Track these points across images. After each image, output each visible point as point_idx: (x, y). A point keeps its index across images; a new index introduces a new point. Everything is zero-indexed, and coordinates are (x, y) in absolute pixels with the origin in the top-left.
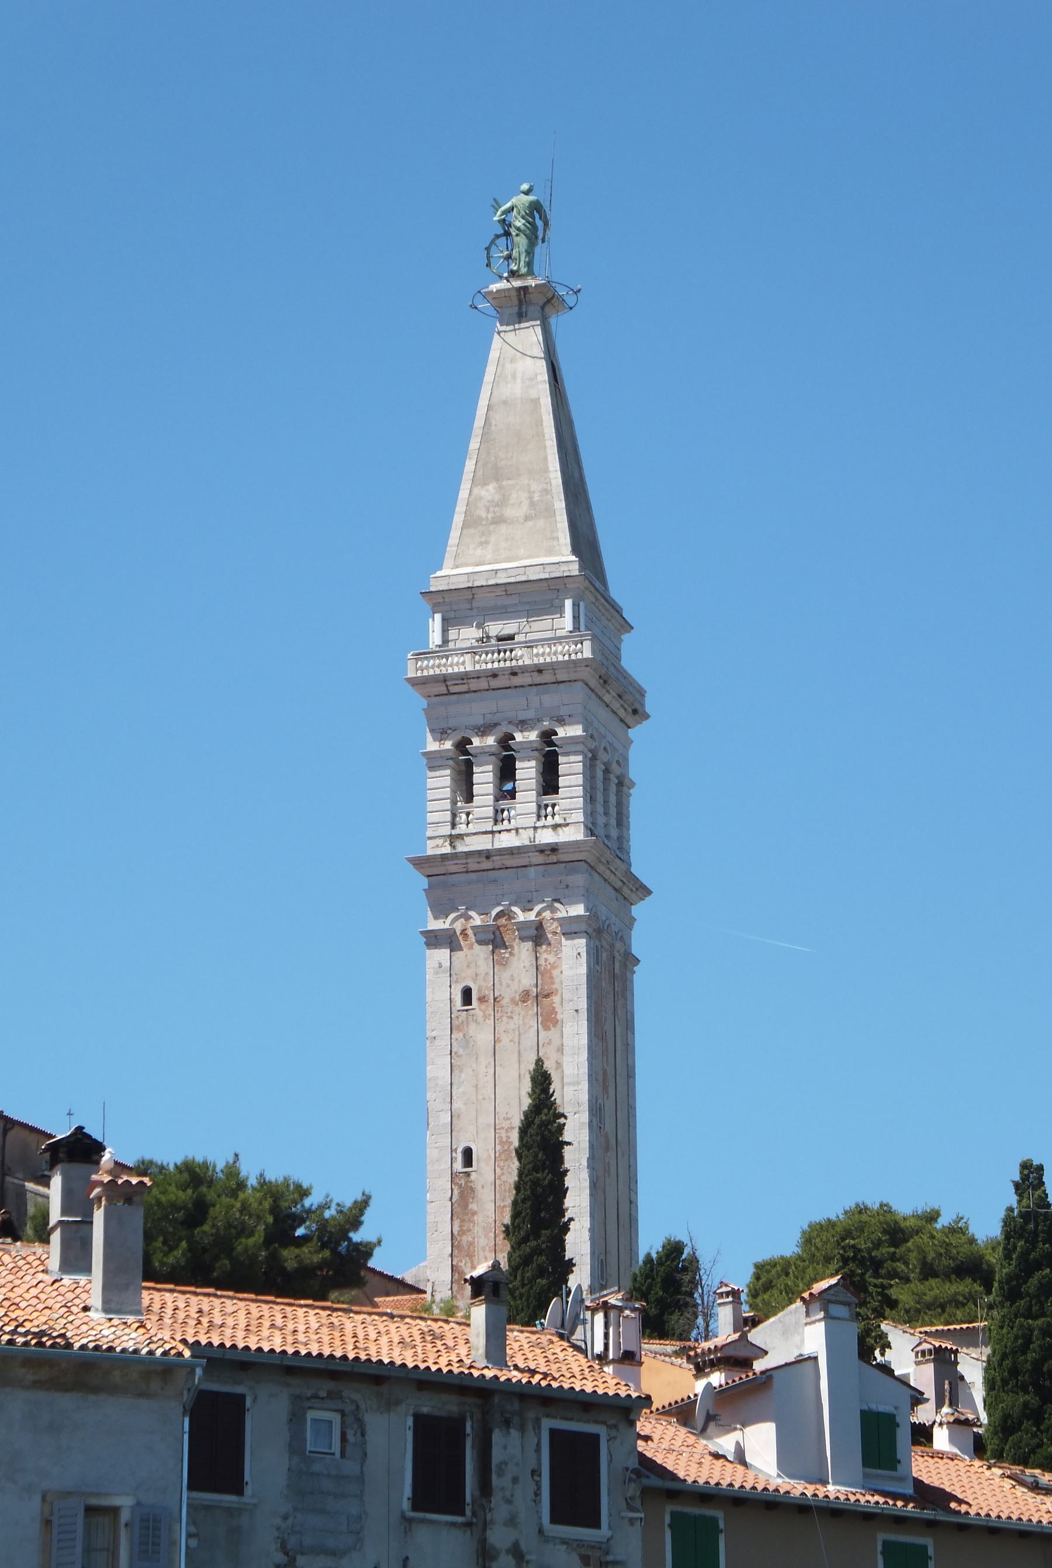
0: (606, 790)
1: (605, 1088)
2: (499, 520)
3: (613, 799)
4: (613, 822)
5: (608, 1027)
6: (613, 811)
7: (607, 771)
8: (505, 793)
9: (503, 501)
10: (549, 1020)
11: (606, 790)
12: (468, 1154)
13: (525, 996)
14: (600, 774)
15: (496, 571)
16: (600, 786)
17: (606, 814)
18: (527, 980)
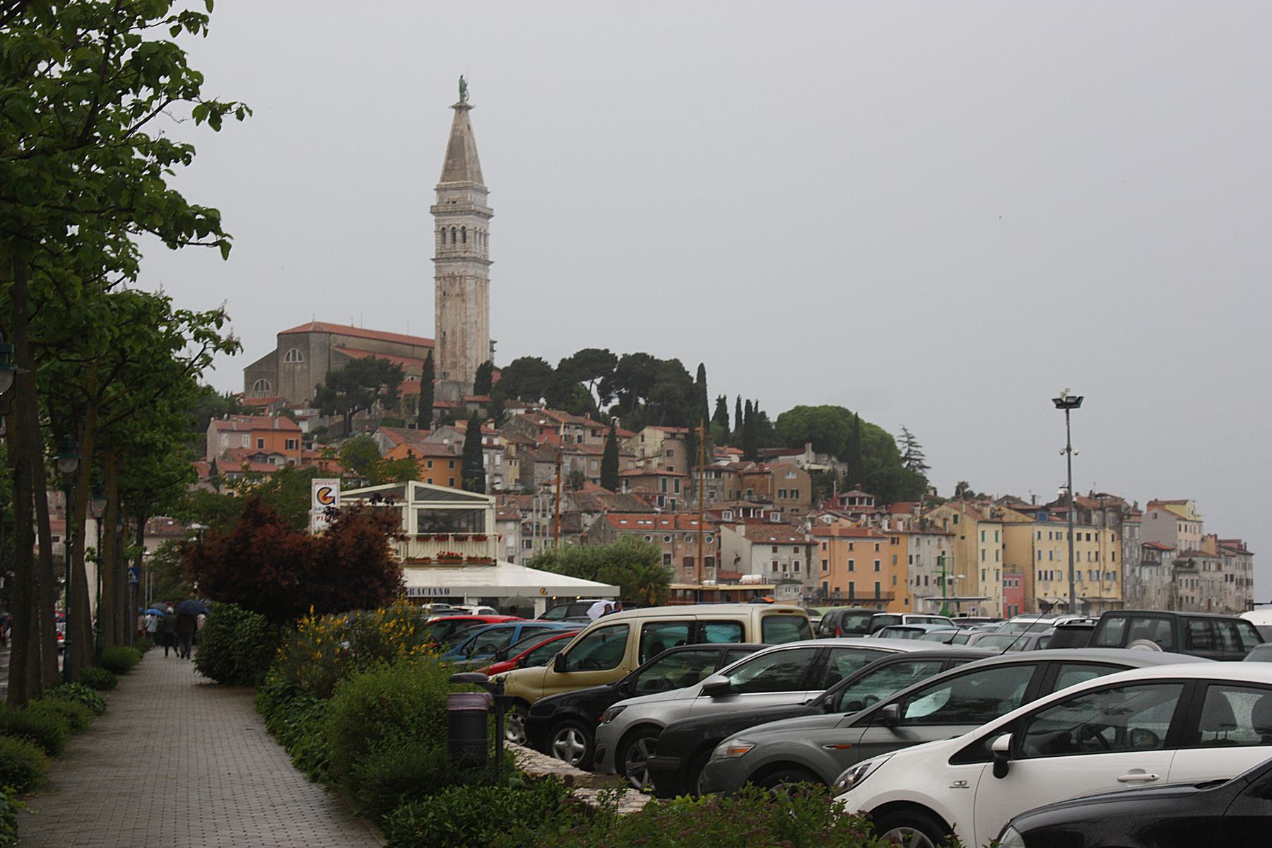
0: (480, 238)
1: (478, 316)
2: (453, 169)
3: (482, 240)
4: (482, 246)
5: (480, 301)
6: (482, 243)
7: (481, 234)
8: (454, 240)
9: (453, 165)
10: (463, 301)
11: (480, 238)
12: (444, 333)
13: (458, 295)
14: (478, 236)
15: (451, 185)
16: (478, 238)
17: (480, 244)
18: (458, 291)
